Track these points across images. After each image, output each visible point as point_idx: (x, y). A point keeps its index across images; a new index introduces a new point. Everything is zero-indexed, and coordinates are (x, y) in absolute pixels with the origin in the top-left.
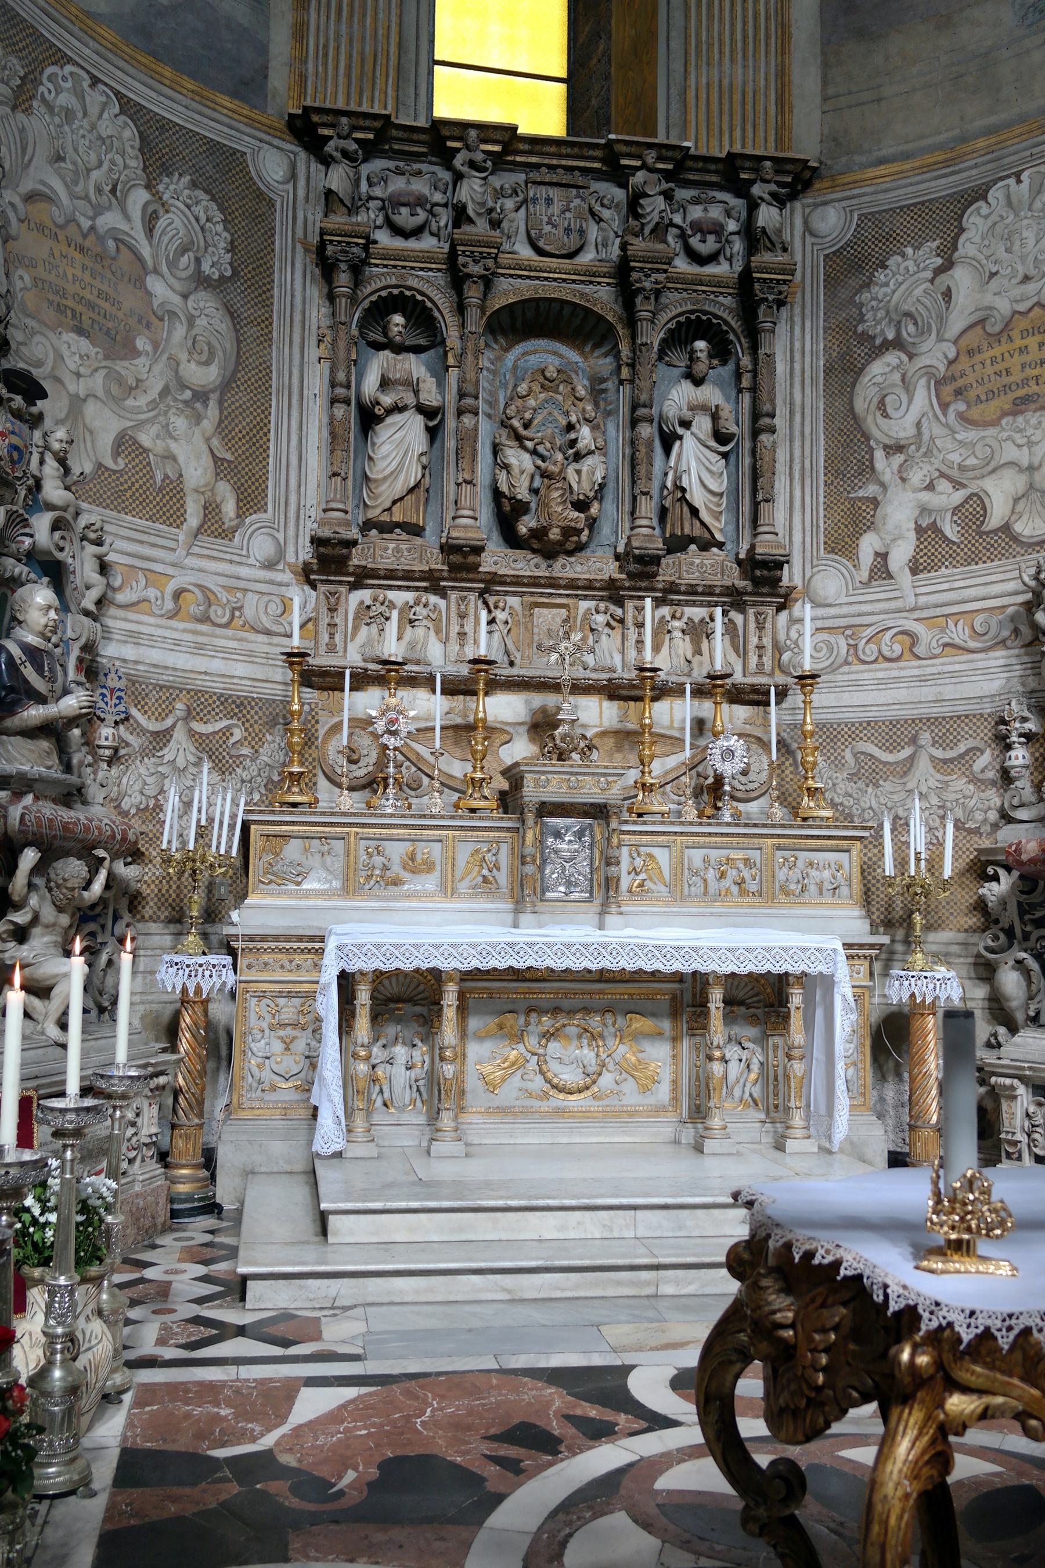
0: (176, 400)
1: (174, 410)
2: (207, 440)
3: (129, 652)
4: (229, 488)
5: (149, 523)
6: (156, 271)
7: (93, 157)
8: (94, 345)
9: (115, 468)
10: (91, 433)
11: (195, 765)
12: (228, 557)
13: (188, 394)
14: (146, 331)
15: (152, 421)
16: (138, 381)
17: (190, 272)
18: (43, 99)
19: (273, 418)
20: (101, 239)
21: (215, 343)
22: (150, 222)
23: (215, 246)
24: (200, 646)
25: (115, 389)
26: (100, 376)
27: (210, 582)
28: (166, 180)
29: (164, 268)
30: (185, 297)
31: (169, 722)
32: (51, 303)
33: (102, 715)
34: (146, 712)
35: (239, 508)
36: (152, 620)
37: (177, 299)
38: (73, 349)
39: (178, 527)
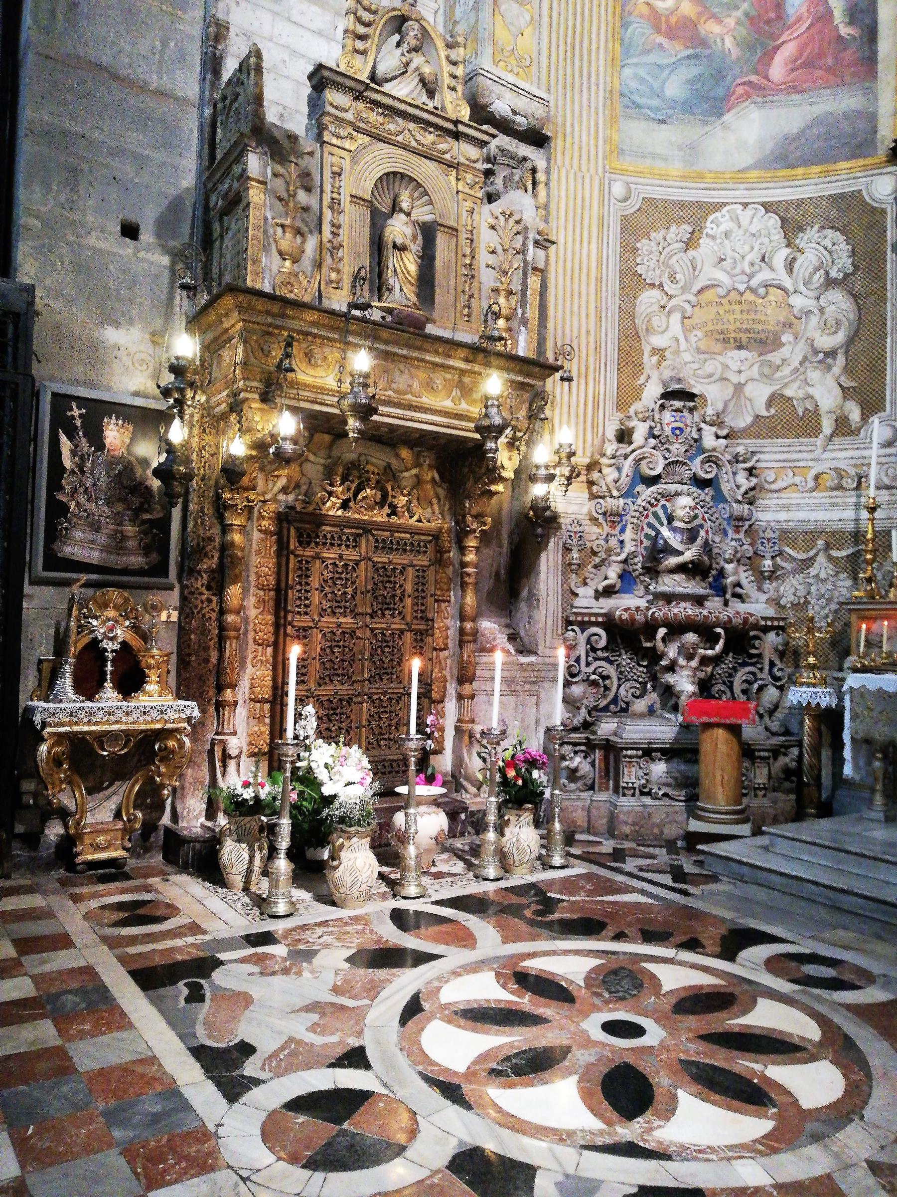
0: (811, 362)
2: (837, 380)
3: (783, 516)
4: (854, 403)
6: (795, 292)
7: (747, 248)
10: (750, 400)
11: (834, 576)
13: (821, 356)
16: (783, 360)
17: (821, 281)
18: (708, 235)
20: (754, 291)
22: (790, 266)
23: (840, 258)
24: (835, 505)
25: (767, 371)
26: (755, 368)
27: (841, 465)
28: (801, 235)
29: (802, 288)
30: (817, 298)
31: (812, 553)
32: (718, 340)
35: (863, 414)
36: (799, 495)
37: (813, 302)
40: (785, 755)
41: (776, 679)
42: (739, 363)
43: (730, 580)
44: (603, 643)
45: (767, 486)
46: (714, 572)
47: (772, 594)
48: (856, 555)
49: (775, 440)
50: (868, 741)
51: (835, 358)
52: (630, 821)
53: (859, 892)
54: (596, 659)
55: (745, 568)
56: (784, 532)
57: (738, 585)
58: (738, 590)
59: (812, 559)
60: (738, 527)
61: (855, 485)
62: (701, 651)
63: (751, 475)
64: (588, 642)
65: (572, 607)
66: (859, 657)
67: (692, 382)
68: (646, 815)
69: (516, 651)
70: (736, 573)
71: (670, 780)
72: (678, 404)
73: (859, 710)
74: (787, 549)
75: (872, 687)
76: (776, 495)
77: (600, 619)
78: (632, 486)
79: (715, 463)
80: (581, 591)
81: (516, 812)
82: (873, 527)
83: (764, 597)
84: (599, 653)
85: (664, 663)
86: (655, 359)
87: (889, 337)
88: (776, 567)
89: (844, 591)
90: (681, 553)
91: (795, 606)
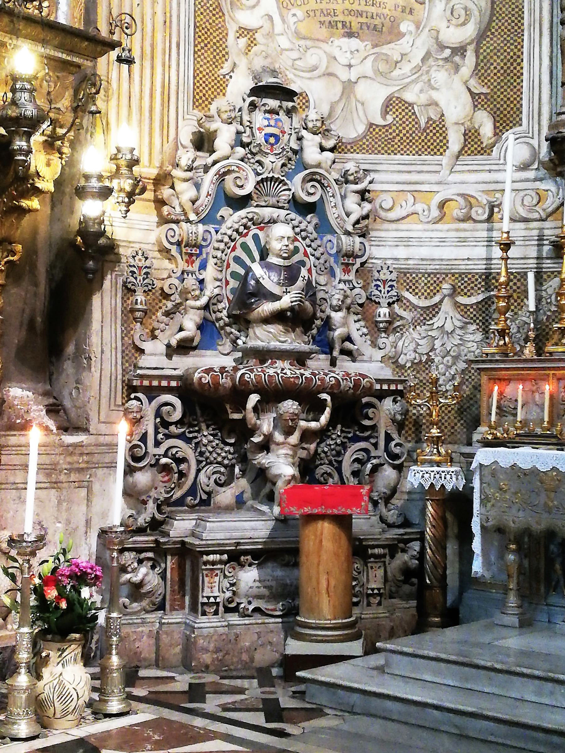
1: (435, 68)
2: (465, 83)
3: (401, 252)
5: (416, 157)
8: (362, 41)
9: (384, 123)
11: (461, 328)
12: (487, 167)
13: (448, 52)
14: (410, 17)
15: (415, 81)
16: (402, 55)
19: (525, 50)
21: (471, 5)
24: (463, 240)
25: (382, 67)
27: (470, 190)
31: (437, 299)
33: (377, 300)
34: (417, 294)
35: (495, 127)
36: (420, 227)
38: (344, 50)
39: (441, 154)
40: (404, 551)
41: (395, 457)
42: (348, 55)
43: (338, 333)
44: (177, 415)
45: (383, 214)
46: (318, 322)
47: (389, 350)
48: (487, 302)
49: (392, 156)
50: (500, 530)
51: (463, 56)
52: (212, 646)
53: (490, 714)
54: (168, 436)
55: (356, 318)
56: (403, 273)
57: (349, 339)
58: (348, 345)
59: (437, 307)
60: (347, 265)
61: (486, 216)
62: (303, 424)
63: (363, 199)
64: (158, 414)
65: (136, 367)
66: (490, 427)
67: (290, 76)
68: (232, 637)
69: (58, 428)
70: (345, 324)
71: (264, 591)
72: (273, 103)
73: (490, 491)
74: (407, 295)
75: (505, 463)
76: (394, 226)
77: (174, 384)
78: (215, 208)
79: (319, 182)
80: (147, 346)
81: (58, 645)
82: (507, 269)
83: (379, 355)
84: (173, 428)
85: (256, 439)
86: (243, 42)
87: (526, 33)
88: (394, 317)
89: (473, 347)
90: (279, 298)
91: (417, 365)
